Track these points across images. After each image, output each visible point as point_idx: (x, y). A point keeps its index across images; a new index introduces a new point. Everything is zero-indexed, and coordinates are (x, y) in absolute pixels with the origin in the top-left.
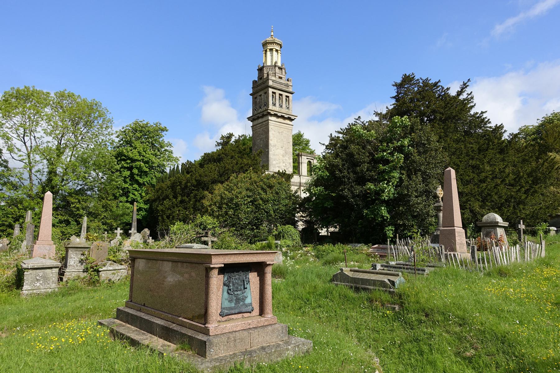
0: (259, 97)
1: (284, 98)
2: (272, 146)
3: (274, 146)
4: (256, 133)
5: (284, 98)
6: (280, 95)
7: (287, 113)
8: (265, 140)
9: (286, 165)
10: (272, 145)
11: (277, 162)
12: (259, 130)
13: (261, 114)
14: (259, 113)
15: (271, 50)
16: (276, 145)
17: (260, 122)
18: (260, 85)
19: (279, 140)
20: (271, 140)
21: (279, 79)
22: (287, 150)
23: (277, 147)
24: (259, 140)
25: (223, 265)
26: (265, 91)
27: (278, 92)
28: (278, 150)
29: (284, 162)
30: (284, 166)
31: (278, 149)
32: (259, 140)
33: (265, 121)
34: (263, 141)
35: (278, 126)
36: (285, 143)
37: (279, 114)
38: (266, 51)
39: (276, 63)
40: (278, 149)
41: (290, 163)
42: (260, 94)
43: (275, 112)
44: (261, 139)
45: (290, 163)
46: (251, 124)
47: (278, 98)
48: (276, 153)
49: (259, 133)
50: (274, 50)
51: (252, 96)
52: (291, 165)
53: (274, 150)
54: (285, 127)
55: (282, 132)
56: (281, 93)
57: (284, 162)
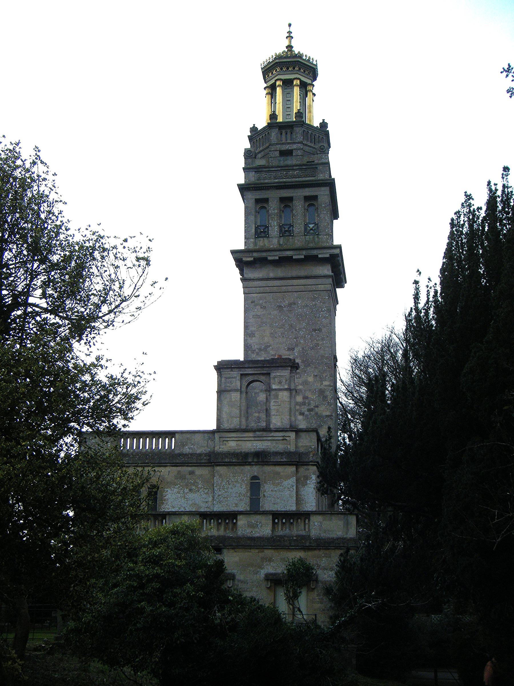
9: (305, 398)
27: (274, 196)
36: (302, 333)
39: (300, 114)
43: (255, 255)
50: (296, 82)
55: (290, 305)
56: (286, 193)
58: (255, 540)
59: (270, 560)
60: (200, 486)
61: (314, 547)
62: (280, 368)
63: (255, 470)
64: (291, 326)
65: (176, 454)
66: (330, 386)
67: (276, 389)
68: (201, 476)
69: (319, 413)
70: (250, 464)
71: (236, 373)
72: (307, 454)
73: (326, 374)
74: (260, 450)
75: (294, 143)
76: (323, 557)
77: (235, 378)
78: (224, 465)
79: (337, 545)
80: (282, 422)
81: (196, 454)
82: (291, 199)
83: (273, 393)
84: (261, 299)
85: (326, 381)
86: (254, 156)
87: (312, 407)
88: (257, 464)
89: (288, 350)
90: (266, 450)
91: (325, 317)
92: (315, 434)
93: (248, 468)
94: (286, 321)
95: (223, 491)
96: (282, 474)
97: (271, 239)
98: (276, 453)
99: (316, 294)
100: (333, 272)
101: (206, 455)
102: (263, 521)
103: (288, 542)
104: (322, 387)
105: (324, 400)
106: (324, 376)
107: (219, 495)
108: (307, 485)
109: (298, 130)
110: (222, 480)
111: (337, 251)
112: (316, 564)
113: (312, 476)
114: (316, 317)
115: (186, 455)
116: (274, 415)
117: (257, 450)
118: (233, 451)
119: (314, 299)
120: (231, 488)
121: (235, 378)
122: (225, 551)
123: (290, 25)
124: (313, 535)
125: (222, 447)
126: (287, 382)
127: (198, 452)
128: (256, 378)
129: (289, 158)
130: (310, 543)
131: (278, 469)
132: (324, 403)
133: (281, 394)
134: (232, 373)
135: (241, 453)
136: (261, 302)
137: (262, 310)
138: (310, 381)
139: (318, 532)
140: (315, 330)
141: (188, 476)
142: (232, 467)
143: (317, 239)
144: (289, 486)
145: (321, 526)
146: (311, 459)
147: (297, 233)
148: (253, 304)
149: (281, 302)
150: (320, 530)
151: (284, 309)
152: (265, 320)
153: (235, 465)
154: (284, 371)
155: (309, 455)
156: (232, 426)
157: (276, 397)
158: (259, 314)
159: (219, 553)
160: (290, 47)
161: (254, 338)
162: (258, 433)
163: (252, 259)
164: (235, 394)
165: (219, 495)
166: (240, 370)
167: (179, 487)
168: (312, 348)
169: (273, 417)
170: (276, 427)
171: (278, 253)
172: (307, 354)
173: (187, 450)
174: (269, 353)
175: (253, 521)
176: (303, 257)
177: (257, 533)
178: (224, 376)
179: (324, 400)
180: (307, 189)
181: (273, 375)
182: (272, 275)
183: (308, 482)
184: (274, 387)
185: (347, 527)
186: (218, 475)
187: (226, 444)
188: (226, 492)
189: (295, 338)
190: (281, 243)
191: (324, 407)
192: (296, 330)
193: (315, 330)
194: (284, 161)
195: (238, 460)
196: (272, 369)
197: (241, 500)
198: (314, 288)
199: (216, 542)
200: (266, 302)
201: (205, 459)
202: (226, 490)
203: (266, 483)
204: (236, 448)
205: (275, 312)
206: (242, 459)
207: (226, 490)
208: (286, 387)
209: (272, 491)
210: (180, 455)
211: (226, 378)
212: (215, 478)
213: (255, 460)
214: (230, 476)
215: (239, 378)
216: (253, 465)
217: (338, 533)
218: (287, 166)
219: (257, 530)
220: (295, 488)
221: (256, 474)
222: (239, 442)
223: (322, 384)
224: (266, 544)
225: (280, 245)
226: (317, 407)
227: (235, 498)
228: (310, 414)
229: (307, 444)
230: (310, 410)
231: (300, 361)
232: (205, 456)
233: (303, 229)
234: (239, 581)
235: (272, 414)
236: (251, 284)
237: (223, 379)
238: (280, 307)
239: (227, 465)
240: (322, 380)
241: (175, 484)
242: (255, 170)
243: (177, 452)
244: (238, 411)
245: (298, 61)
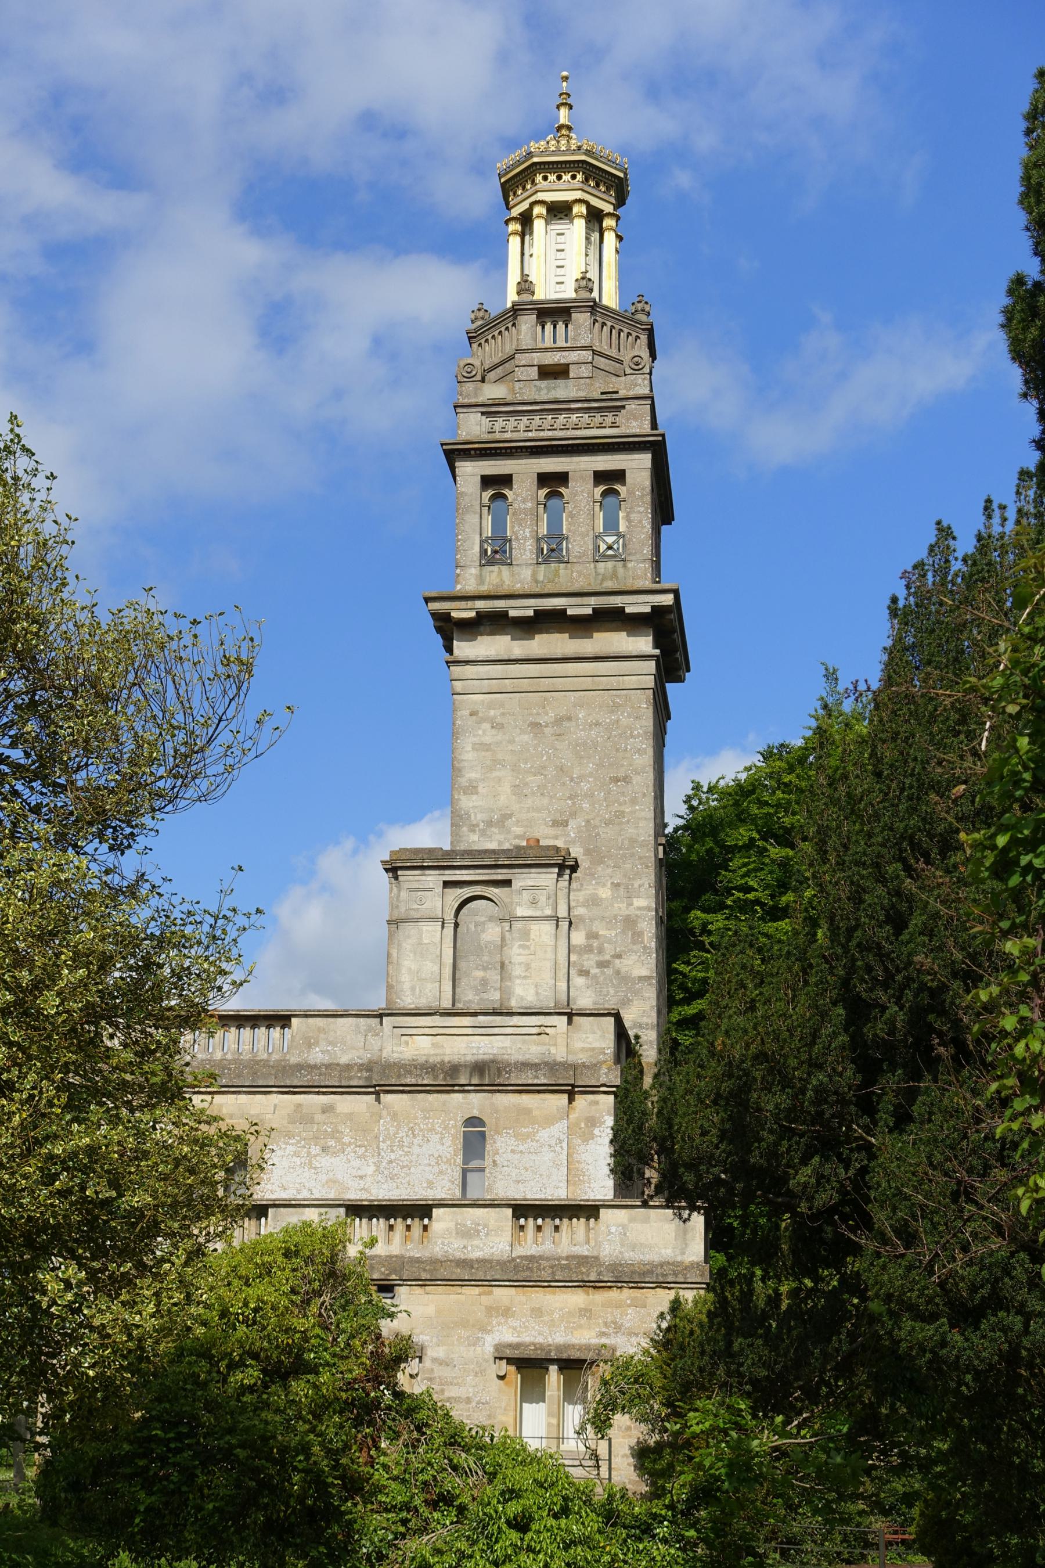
9: (592, 936)
19: (534, 781)
22: (607, 833)
35: (525, 684)
43: (480, 604)
45: (629, 922)
50: (579, 209)
52: (637, 936)
55: (559, 721)
58: (472, 1267)
59: (506, 1312)
60: (346, 1140)
61: (609, 1284)
62: (533, 870)
63: (475, 1103)
65: (290, 1066)
66: (648, 909)
68: (350, 1116)
69: (623, 970)
70: (463, 1089)
71: (433, 879)
72: (594, 1067)
73: (639, 882)
74: (486, 1057)
76: (629, 1306)
77: (430, 890)
78: (403, 1092)
79: (661, 1279)
80: (537, 993)
81: (338, 1065)
82: (562, 478)
83: (518, 925)
84: (491, 706)
85: (639, 897)
86: (479, 377)
87: (607, 957)
88: (479, 1088)
89: (553, 825)
90: (499, 1058)
91: (639, 751)
92: (611, 1020)
93: (458, 1097)
94: (549, 758)
95: (401, 1153)
96: (535, 1113)
97: (515, 568)
98: (525, 1065)
99: (618, 696)
100: (656, 646)
101: (362, 1067)
102: (492, 1224)
103: (550, 1271)
104: (631, 911)
106: (636, 886)
107: (391, 1162)
108: (593, 1139)
109: (582, 319)
110: (398, 1127)
111: (668, 599)
112: (612, 1322)
113: (606, 1118)
114: (617, 750)
115: (315, 1067)
116: (519, 977)
117: (481, 1057)
118: (422, 1060)
119: (614, 708)
120: (420, 1146)
121: (430, 890)
122: (402, 1291)
124: (605, 1256)
125: (400, 1049)
126: (551, 901)
127: (344, 1060)
128: (478, 890)
129: (561, 382)
130: (599, 1274)
131: (526, 1099)
132: (635, 947)
133: (535, 927)
134: (423, 878)
135: (442, 1063)
136: (492, 713)
137: (494, 732)
138: (604, 896)
139: (618, 1248)
140: (616, 780)
141: (319, 1117)
144: (553, 1142)
145: (625, 1234)
146: (603, 1080)
147: (576, 557)
148: (474, 717)
149: (538, 714)
150: (622, 1245)
151: (547, 731)
152: (500, 756)
154: (543, 876)
155: (600, 1068)
156: (422, 1002)
157: (526, 935)
158: (487, 739)
159: (390, 1295)
161: (474, 797)
162: (481, 1018)
163: (472, 614)
164: (430, 928)
165: (391, 1162)
166: (442, 872)
167: (299, 1142)
168: (608, 823)
169: (518, 981)
170: (525, 1004)
171: (532, 602)
172: (598, 834)
173: (317, 1056)
174: (509, 832)
175: (469, 1222)
177: (479, 1249)
178: (406, 885)
179: (634, 943)
181: (516, 884)
183: (596, 1131)
185: (685, 1239)
186: (389, 1114)
187: (407, 1043)
188: (407, 1154)
189: (570, 798)
190: (541, 578)
191: (634, 957)
192: (572, 780)
193: (616, 780)
194: (549, 389)
195: (436, 1078)
197: (441, 1172)
198: (614, 682)
199: (383, 1269)
200: (503, 714)
201: (360, 1078)
202: (406, 1149)
203: (497, 1132)
204: (432, 1052)
205: (526, 738)
206: (445, 1079)
207: (406, 1149)
208: (548, 912)
209: (513, 1151)
210: (300, 1067)
211: (411, 890)
212: (382, 1121)
213: (475, 1081)
214: (416, 1118)
215: (439, 889)
217: (663, 1251)
219: (475, 1242)
220: (565, 1145)
221: (475, 1113)
223: (632, 904)
224: (497, 1277)
225: (537, 581)
226: (619, 956)
227: (428, 1168)
228: (603, 973)
229: (597, 1045)
230: (602, 965)
231: (581, 850)
232: (361, 1071)
233: (591, 547)
234: (435, 1360)
235: (514, 974)
236: (469, 670)
237: (404, 894)
238: (535, 725)
239: (409, 1092)
240: (630, 896)
241: (289, 1135)
242: (484, 410)
243: (293, 1060)
244: (436, 968)
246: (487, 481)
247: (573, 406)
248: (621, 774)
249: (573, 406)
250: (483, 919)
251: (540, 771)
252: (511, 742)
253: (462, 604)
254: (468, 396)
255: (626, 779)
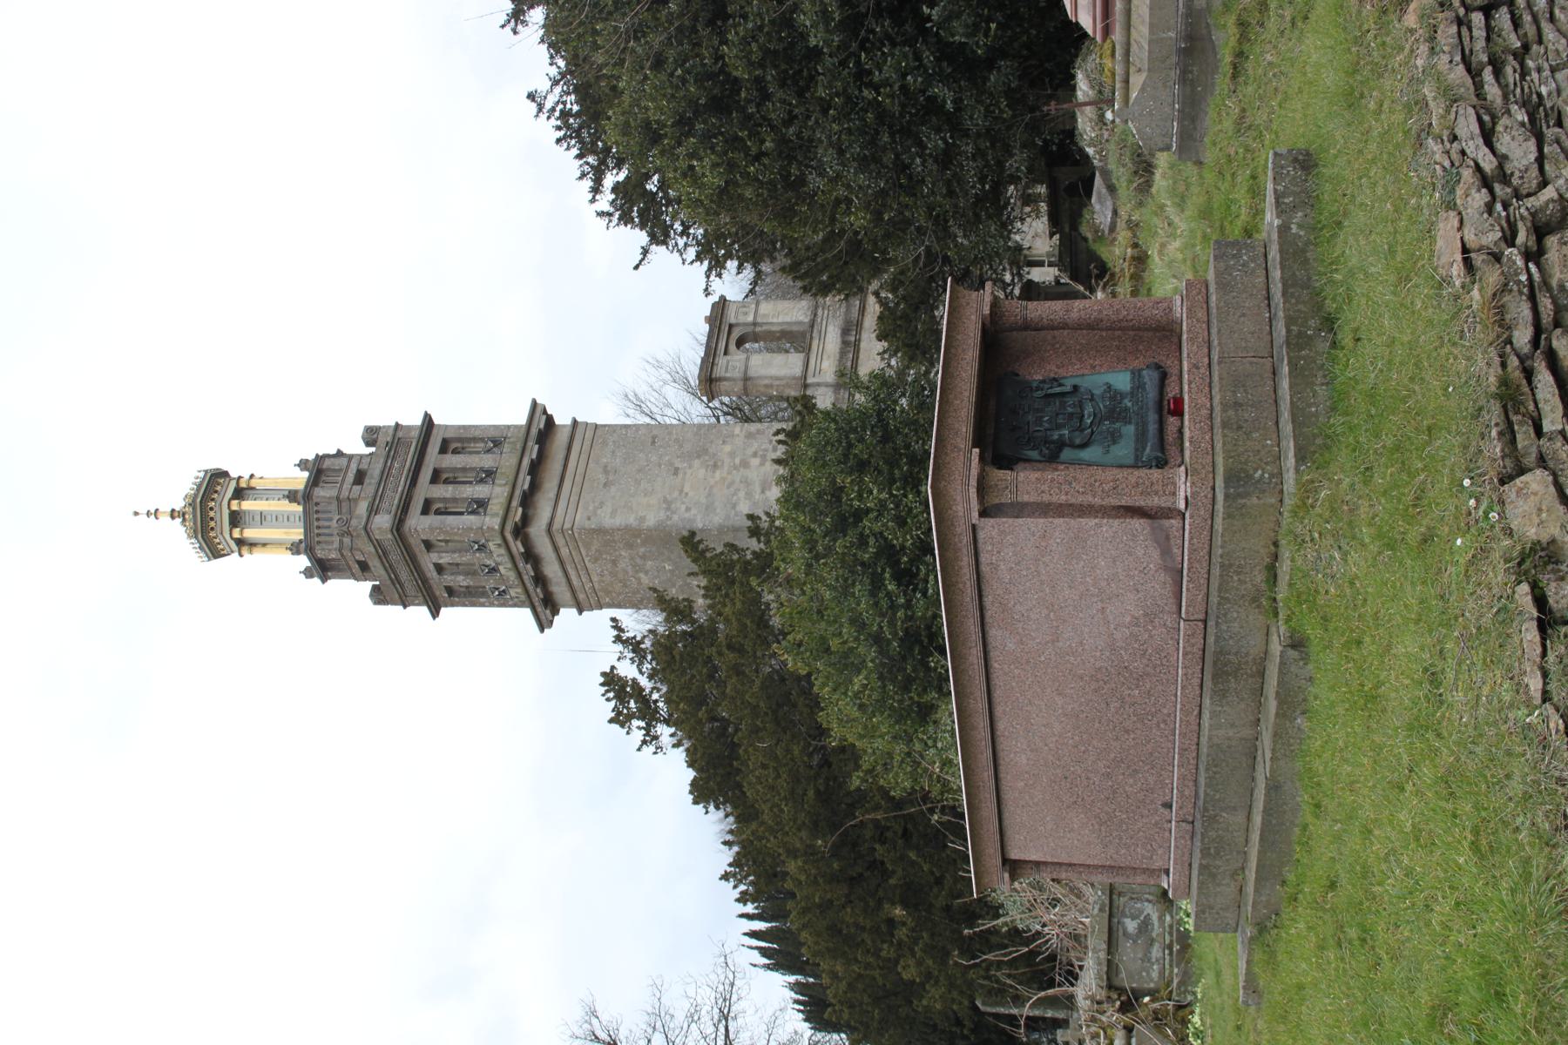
0: (448, 579)
1: (451, 461)
2: (669, 518)
3: (668, 509)
4: (608, 593)
5: (451, 461)
6: (436, 477)
7: (519, 446)
8: (642, 550)
9: (755, 455)
10: (662, 515)
11: (742, 494)
12: (595, 579)
13: (521, 565)
14: (519, 575)
15: (236, 519)
16: (665, 500)
17: (560, 573)
18: (390, 568)
20: (642, 519)
21: (367, 481)
22: (687, 447)
23: (676, 494)
24: (642, 575)
25: (976, 451)
26: (419, 549)
27: (424, 489)
28: (686, 490)
29: (745, 464)
30: (762, 464)
31: (681, 491)
32: (642, 575)
33: (556, 549)
34: (643, 557)
35: (576, 490)
36: (654, 458)
37: (525, 482)
38: (241, 542)
39: (292, 496)
40: (681, 491)
41: (750, 436)
42: (431, 573)
43: (515, 503)
44: (638, 569)
46: (567, 615)
47: (451, 488)
48: (703, 500)
49: (608, 579)
50: (235, 505)
51: (443, 610)
52: (758, 432)
53: (688, 509)
54: (584, 457)
55: (606, 471)
56: (426, 474)
57: (745, 464)
64: (639, 471)
67: (755, 317)
75: (348, 467)
77: (728, 362)
93: (863, 345)
105: (763, 433)
118: (837, 363)
119: (605, 443)
121: (728, 362)
123: (136, 514)
136: (591, 508)
137: (604, 508)
142: (859, 362)
143: (512, 440)
153: (857, 358)
158: (609, 510)
160: (173, 514)
161: (648, 517)
168: (681, 446)
171: (521, 476)
174: (676, 499)
176: (537, 447)
179: (763, 433)
180: (429, 450)
181: (733, 321)
182: (552, 495)
184: (750, 318)
190: (504, 482)
195: (849, 352)
196: (724, 320)
198: (587, 443)
215: (728, 357)
216: (860, 339)
218: (383, 473)
222: (824, 357)
225: (506, 484)
245: (201, 502)
246: (426, 511)
247: (389, 464)
248: (650, 440)
249: (389, 464)
250: (733, 512)
251: (638, 482)
252: (613, 498)
253: (511, 514)
254: (360, 523)
255: (654, 438)
